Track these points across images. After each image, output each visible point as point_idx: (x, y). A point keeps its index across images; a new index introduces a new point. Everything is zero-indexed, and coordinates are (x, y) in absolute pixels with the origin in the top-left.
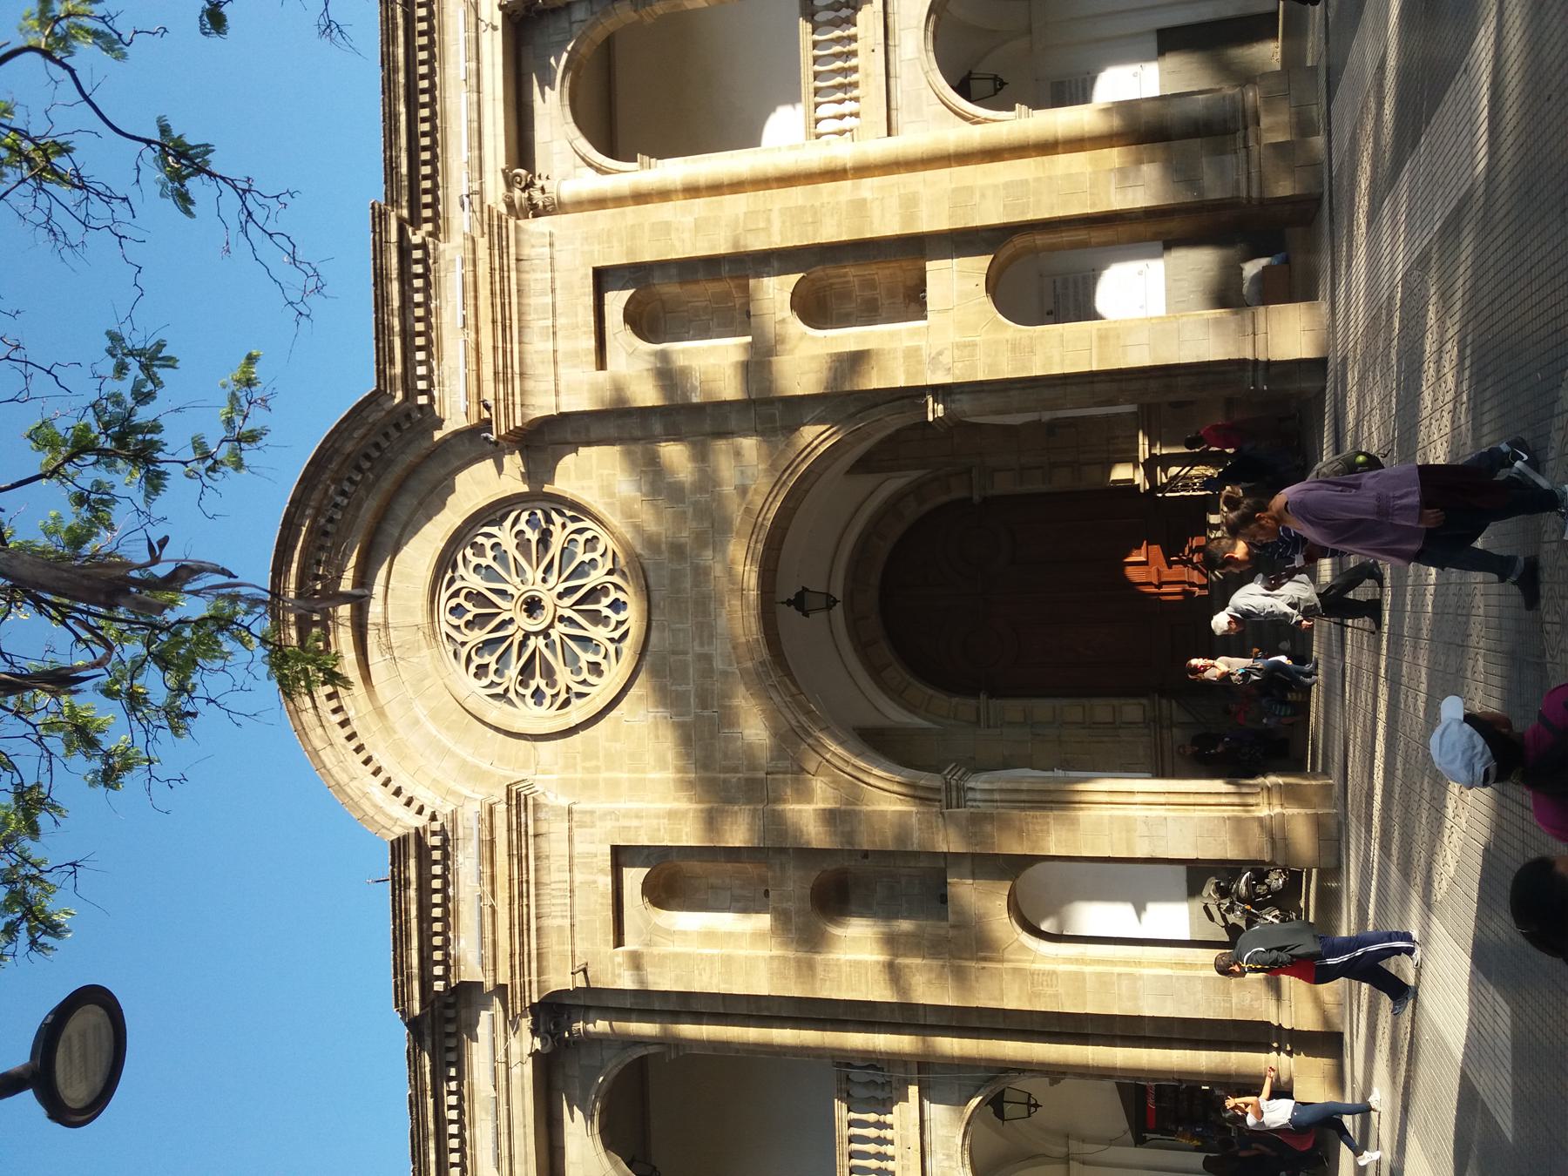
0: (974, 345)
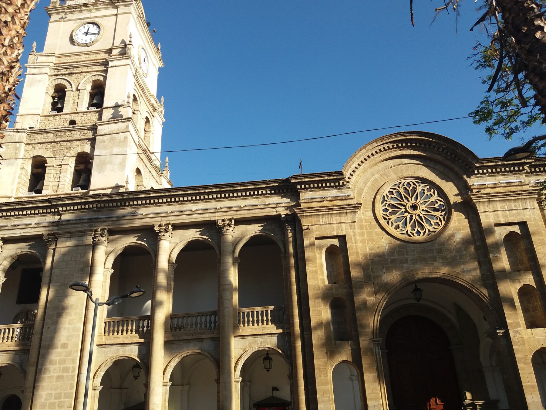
0: (524, 345)
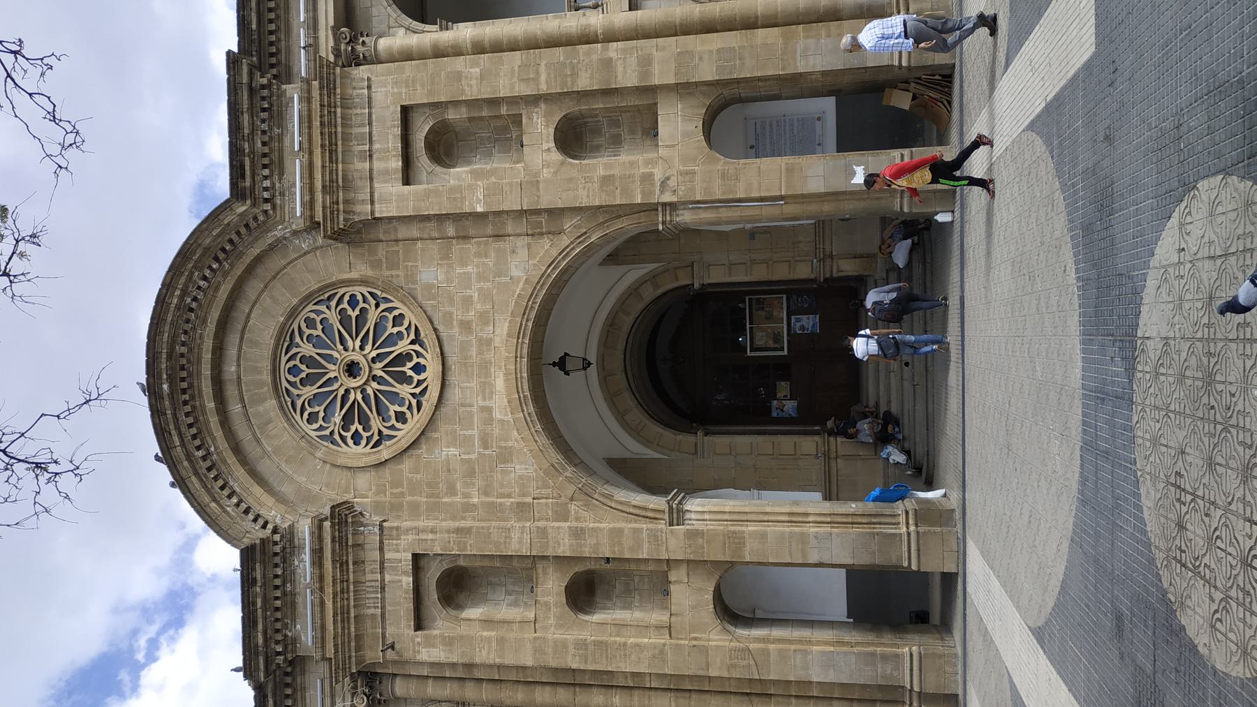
0: (694, 173)
